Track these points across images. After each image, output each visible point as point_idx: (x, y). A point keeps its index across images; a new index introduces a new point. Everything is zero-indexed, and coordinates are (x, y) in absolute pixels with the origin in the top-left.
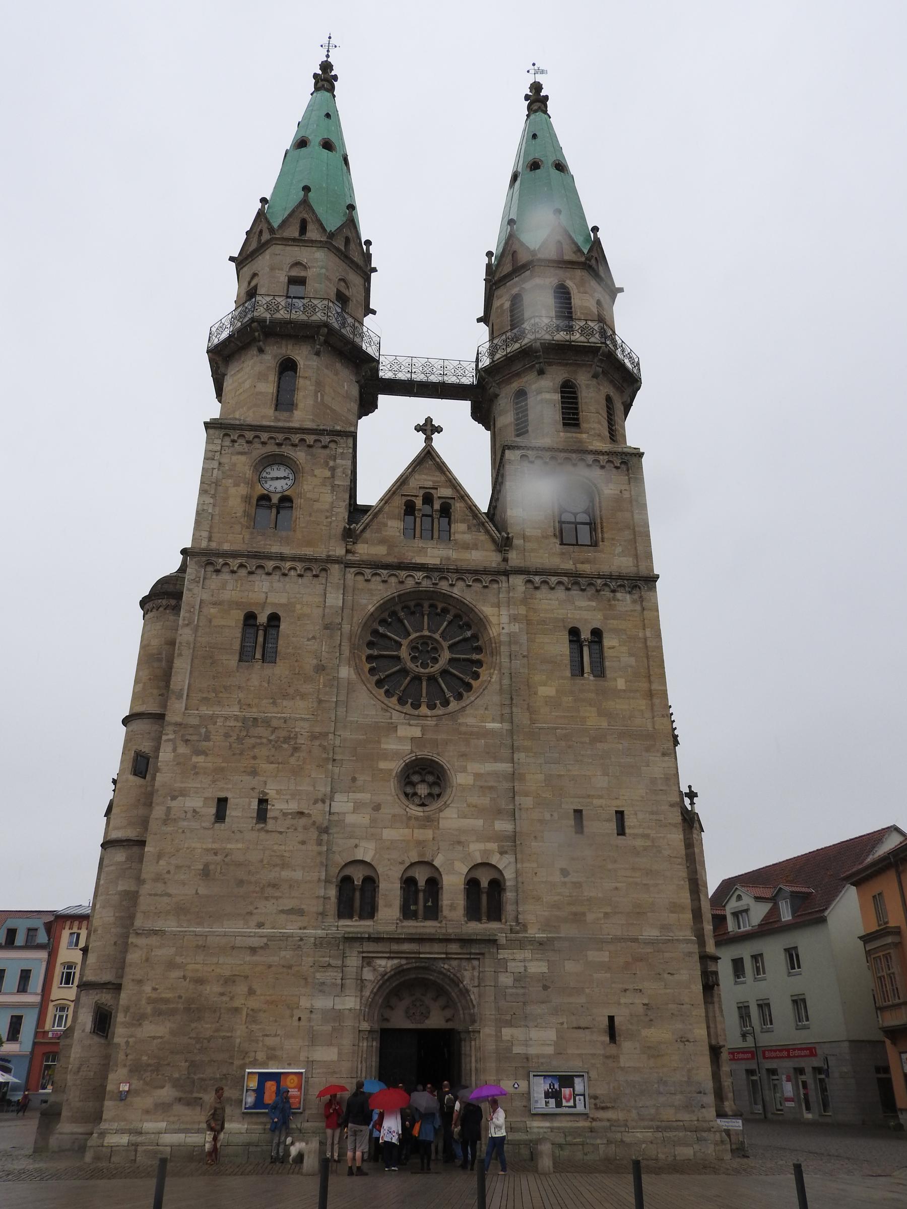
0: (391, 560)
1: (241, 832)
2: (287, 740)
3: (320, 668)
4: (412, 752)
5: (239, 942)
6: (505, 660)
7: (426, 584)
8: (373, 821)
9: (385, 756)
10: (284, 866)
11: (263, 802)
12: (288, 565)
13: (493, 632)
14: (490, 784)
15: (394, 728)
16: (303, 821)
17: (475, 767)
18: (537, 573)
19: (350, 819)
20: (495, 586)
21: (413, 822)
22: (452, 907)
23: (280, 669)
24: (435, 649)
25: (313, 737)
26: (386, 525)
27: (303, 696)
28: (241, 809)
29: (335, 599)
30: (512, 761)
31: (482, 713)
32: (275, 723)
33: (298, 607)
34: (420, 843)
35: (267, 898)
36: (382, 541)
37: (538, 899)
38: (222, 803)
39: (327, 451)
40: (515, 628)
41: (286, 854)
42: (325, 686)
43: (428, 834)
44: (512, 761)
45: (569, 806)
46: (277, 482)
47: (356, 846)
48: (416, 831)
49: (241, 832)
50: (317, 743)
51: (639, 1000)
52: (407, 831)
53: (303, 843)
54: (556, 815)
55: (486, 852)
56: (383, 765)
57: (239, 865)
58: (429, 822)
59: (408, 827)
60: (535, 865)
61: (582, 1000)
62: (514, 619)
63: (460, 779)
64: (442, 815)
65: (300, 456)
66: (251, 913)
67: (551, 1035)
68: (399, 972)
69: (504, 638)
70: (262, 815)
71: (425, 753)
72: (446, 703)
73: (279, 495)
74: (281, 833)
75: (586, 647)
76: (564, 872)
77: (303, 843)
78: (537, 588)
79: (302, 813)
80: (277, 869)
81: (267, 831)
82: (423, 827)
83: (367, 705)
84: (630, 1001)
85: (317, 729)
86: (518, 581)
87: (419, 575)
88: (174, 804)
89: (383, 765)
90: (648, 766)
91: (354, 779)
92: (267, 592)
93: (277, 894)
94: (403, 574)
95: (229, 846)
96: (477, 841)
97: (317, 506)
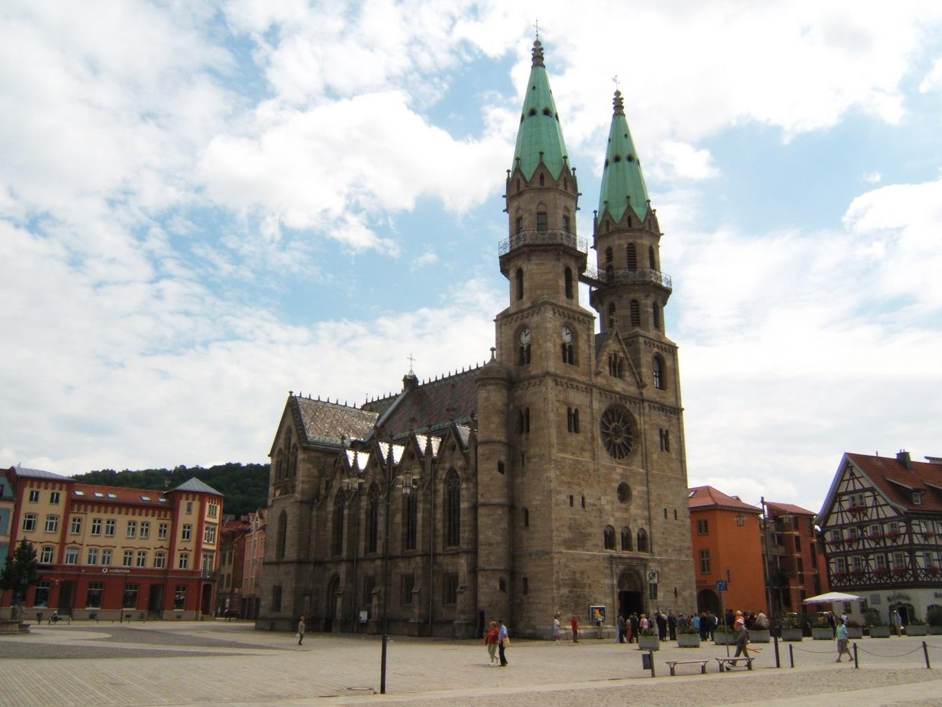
4: (621, 479)
8: (613, 508)
15: (614, 468)
16: (595, 508)
22: (635, 545)
28: (578, 501)
30: (648, 487)
34: (625, 519)
38: (571, 498)
44: (648, 487)
45: (664, 507)
53: (596, 517)
68: (625, 569)
70: (583, 505)
71: (624, 480)
75: (664, 436)
77: (596, 517)
82: (626, 512)
83: (605, 458)
88: (558, 497)
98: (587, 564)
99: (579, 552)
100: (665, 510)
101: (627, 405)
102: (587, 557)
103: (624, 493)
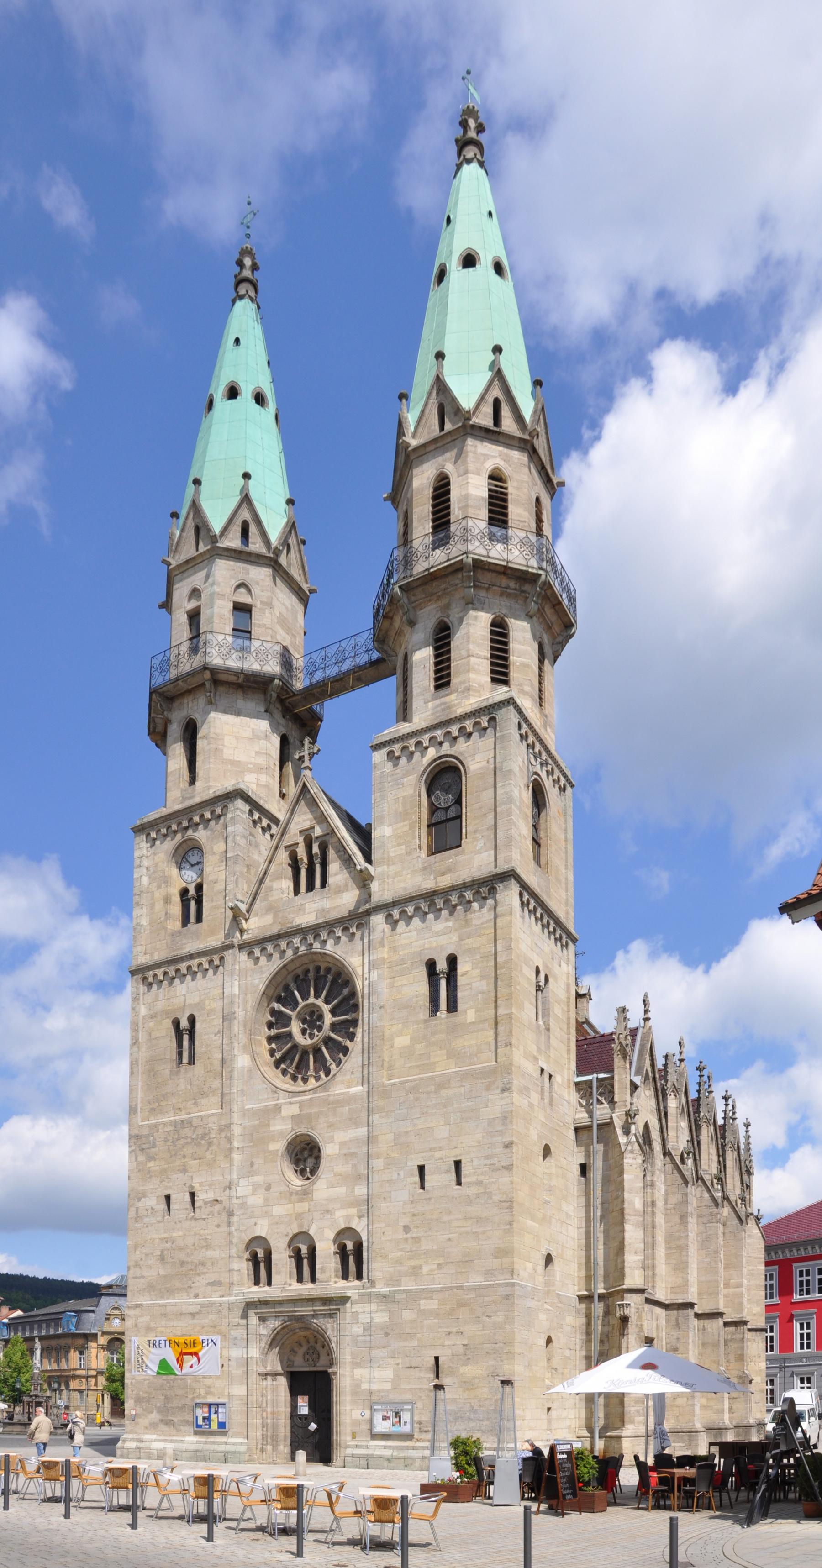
1: (180, 1222)
4: (293, 1130)
5: (184, 1309)
9: (273, 1139)
10: (208, 1247)
11: (192, 1195)
14: (352, 1151)
16: (218, 1207)
17: (341, 1136)
19: (251, 1201)
21: (294, 1197)
31: (346, 1081)
34: (299, 1216)
35: (199, 1274)
37: (385, 1257)
41: (209, 1237)
43: (305, 1206)
47: (255, 1224)
48: (296, 1205)
49: (180, 1222)
51: (460, 1341)
52: (290, 1206)
53: (218, 1226)
54: (402, 1173)
55: (349, 1217)
56: (272, 1147)
57: (181, 1249)
58: (305, 1194)
59: (290, 1202)
60: (383, 1225)
61: (415, 1343)
63: (328, 1150)
64: (315, 1187)
66: (190, 1287)
67: (389, 1374)
71: (301, 1129)
74: (204, 1219)
76: (407, 1229)
77: (218, 1226)
79: (217, 1200)
80: (204, 1250)
81: (196, 1219)
82: (301, 1201)
84: (453, 1343)
89: (272, 1147)
90: (487, 1106)
91: (252, 1164)
93: (205, 1270)
95: (174, 1234)
96: (342, 1208)
98: (191, 1322)
99: (181, 1300)
100: (421, 1169)
101: (330, 948)
102: (193, 1309)
103: (305, 1154)
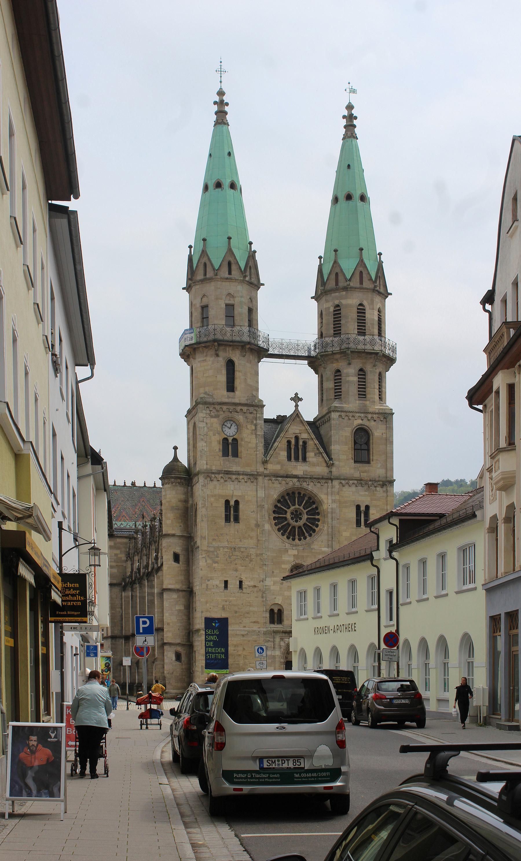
0: (282, 473)
2: (247, 557)
3: (257, 525)
6: (330, 520)
7: (297, 484)
12: (241, 477)
13: (325, 507)
15: (286, 551)
18: (344, 479)
20: (326, 484)
23: (241, 526)
24: (301, 514)
25: (257, 555)
26: (279, 454)
27: (251, 538)
29: (261, 494)
32: (242, 550)
33: (246, 497)
36: (279, 463)
39: (252, 415)
40: (334, 506)
42: (260, 533)
46: (230, 432)
50: (259, 558)
56: (283, 566)
62: (334, 501)
65: (240, 418)
69: (329, 510)
72: (305, 538)
73: (232, 438)
78: (343, 486)
85: (258, 552)
86: (336, 483)
87: (295, 480)
89: (283, 566)
91: (273, 572)
92: (233, 490)
94: (288, 479)
97: (250, 445)
